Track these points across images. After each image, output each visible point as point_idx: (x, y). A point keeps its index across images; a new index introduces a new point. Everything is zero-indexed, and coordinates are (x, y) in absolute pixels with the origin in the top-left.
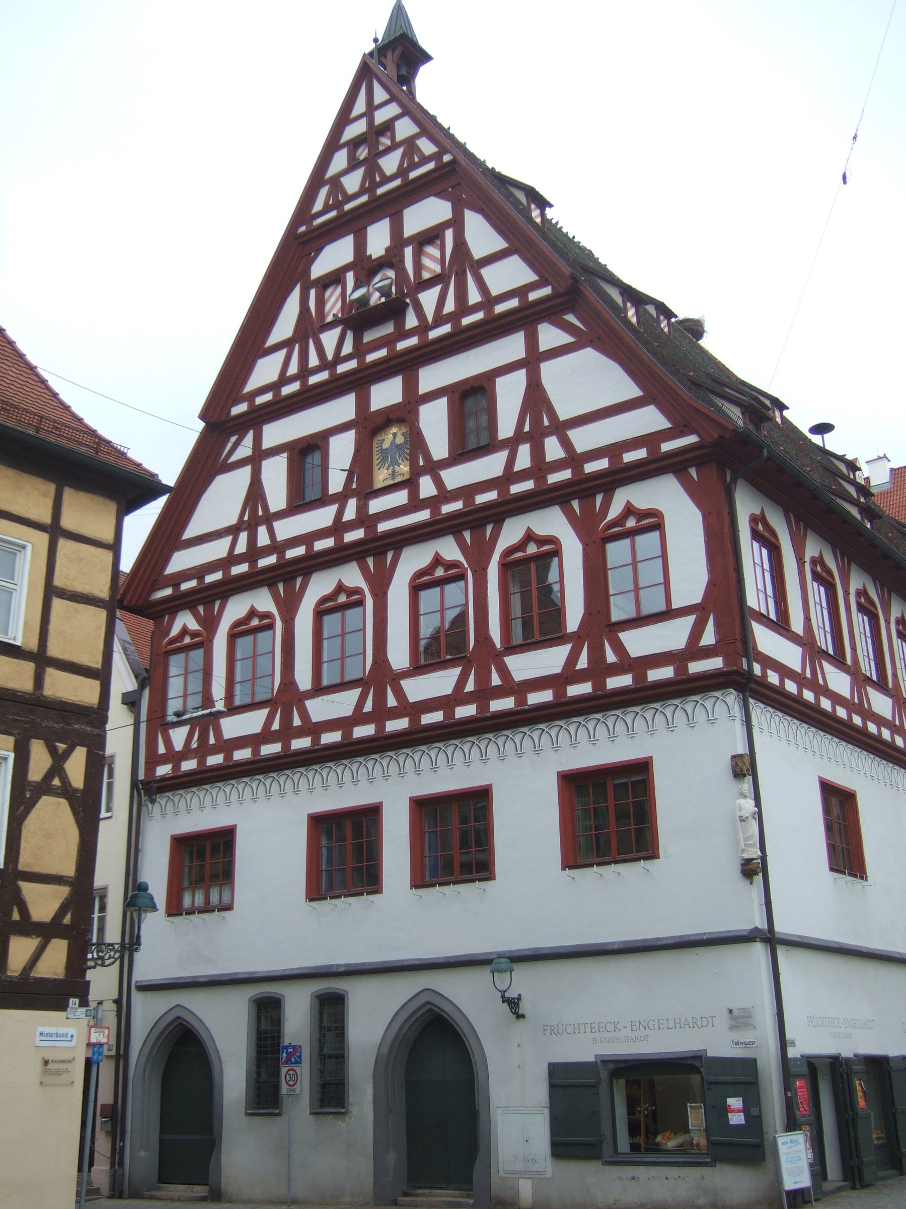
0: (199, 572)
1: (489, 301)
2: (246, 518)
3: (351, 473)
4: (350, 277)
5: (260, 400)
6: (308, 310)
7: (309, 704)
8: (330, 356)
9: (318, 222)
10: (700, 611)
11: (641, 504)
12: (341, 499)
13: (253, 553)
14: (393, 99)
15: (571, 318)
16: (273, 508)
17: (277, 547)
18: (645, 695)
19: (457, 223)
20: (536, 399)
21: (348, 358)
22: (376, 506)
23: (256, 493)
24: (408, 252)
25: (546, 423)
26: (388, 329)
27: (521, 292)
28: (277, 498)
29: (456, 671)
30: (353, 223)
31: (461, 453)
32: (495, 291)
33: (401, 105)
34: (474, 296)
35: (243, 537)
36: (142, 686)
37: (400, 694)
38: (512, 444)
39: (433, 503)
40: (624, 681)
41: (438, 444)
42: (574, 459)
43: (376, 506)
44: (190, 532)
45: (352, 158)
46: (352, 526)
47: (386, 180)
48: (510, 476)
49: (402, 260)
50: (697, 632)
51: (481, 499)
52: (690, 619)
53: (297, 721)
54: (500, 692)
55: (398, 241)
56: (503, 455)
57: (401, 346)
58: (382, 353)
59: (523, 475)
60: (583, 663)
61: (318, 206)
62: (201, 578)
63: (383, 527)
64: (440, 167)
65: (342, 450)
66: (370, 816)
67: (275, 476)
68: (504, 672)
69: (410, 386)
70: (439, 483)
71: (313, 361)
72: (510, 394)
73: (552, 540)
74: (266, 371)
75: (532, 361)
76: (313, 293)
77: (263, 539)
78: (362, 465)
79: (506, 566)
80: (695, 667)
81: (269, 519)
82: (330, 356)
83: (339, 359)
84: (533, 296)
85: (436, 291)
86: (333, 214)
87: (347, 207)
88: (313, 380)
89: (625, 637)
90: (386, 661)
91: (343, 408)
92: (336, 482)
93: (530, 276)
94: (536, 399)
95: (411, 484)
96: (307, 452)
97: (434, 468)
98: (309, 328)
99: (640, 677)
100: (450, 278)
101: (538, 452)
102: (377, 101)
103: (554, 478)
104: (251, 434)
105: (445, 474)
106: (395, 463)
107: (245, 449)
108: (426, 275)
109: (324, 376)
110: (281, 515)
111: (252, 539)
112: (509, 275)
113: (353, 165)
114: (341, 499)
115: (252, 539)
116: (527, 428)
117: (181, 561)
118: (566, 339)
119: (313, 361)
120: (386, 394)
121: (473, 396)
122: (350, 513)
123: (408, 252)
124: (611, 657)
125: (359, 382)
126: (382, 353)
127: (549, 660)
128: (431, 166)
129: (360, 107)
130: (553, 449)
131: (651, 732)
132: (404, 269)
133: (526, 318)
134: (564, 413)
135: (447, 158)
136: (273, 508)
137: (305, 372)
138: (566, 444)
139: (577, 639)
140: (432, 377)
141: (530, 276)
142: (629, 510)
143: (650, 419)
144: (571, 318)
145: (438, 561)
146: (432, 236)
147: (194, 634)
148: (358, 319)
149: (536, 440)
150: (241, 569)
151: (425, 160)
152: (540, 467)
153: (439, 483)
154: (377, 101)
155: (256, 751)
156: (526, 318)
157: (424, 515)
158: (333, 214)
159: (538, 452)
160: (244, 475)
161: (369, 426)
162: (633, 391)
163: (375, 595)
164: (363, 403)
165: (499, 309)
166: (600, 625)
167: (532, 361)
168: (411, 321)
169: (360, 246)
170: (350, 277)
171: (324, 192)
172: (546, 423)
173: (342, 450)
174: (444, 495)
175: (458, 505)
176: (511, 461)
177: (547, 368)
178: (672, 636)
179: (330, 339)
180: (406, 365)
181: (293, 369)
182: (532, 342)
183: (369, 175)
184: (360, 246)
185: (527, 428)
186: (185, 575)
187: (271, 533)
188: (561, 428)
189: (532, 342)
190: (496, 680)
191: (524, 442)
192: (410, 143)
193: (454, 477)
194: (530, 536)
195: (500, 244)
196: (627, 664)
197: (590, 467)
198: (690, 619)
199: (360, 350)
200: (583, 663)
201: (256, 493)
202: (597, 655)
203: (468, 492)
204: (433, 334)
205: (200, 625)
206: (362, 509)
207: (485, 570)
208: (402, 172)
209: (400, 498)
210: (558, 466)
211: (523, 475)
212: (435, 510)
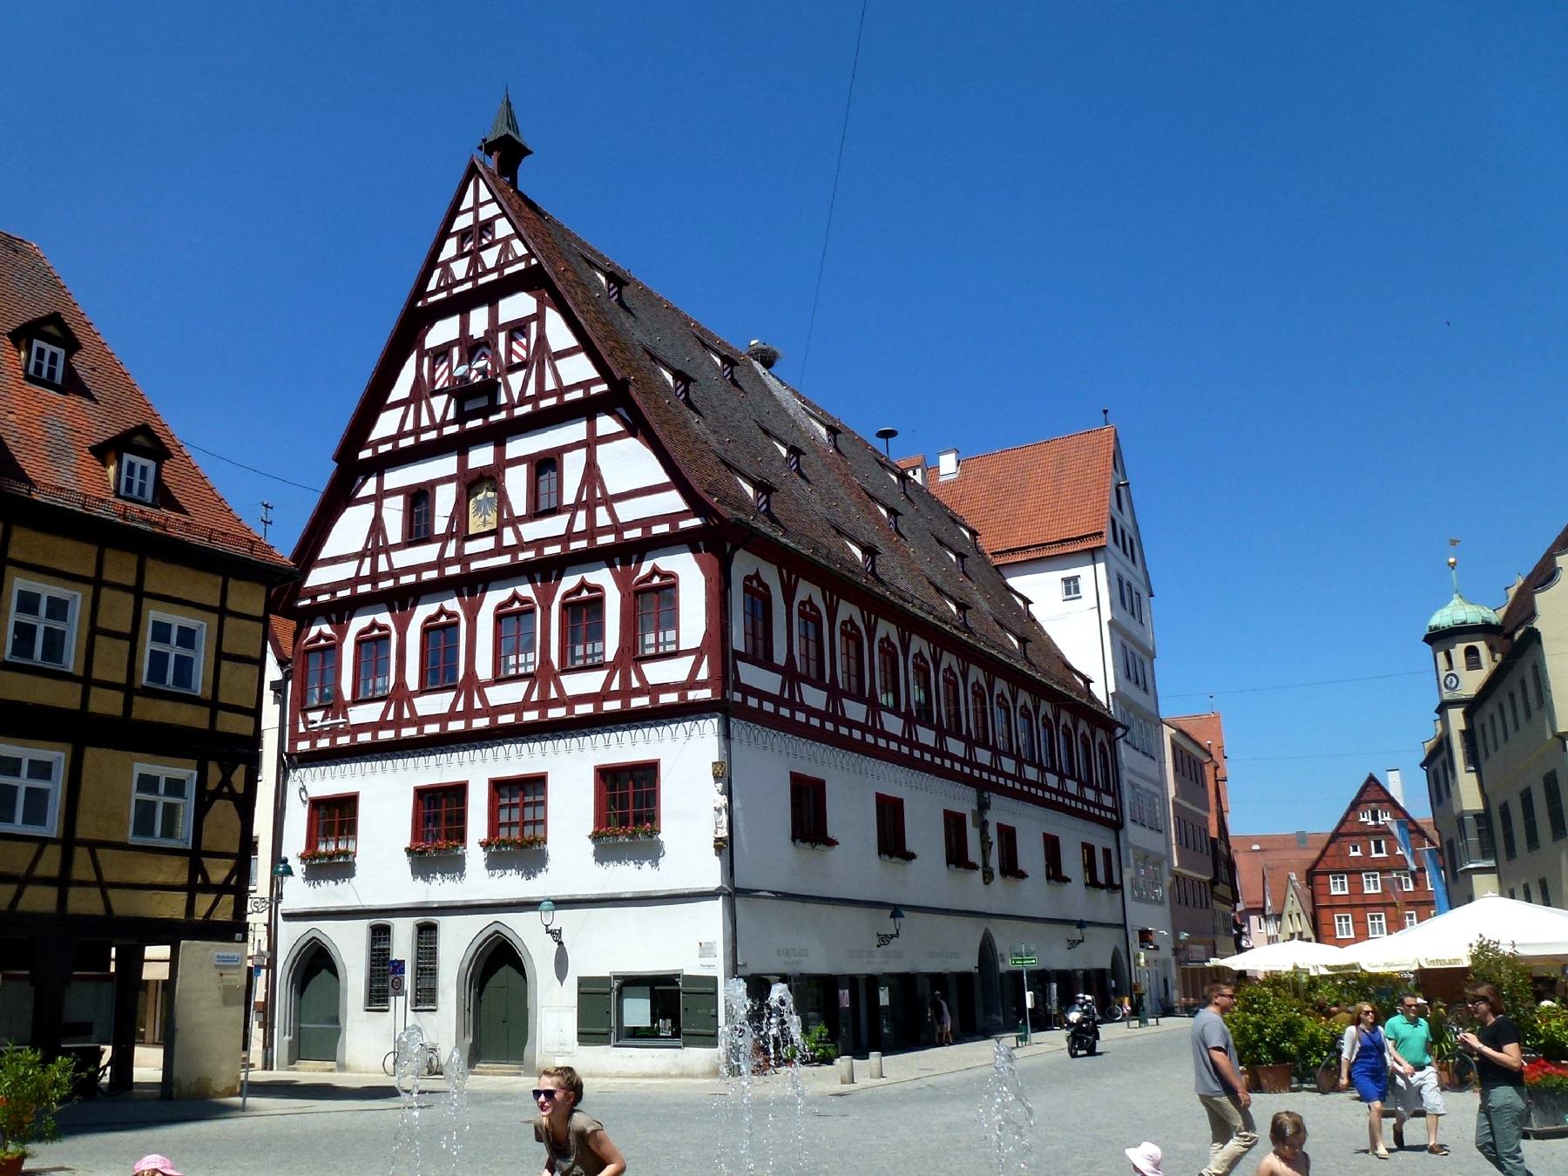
0: (333, 588)
1: (561, 390)
3: (452, 519)
4: (456, 351)
5: (382, 449)
7: (416, 701)
9: (430, 300)
10: (698, 652)
12: (445, 538)
13: (375, 577)
14: (494, 199)
16: (391, 542)
17: (394, 574)
19: (539, 317)
20: (592, 474)
23: (377, 526)
24: (502, 336)
27: (585, 385)
28: (394, 533)
30: (460, 306)
31: (535, 513)
33: (501, 206)
34: (550, 385)
35: (368, 561)
36: (286, 677)
37: (483, 699)
39: (513, 550)
42: (617, 528)
43: (471, 547)
44: (325, 553)
45: (460, 246)
46: (450, 562)
47: (487, 272)
49: (496, 344)
51: (550, 551)
52: (692, 658)
53: (406, 715)
55: (494, 326)
56: (566, 517)
58: (479, 422)
59: (580, 536)
60: (615, 686)
61: (432, 286)
62: (334, 593)
63: (475, 565)
64: (529, 270)
65: (445, 498)
66: (458, 792)
67: (394, 512)
69: (500, 454)
70: (518, 534)
71: (425, 422)
73: (598, 588)
75: (591, 443)
77: (383, 566)
78: (460, 512)
79: (564, 607)
80: (692, 695)
81: (388, 549)
83: (445, 423)
84: (594, 390)
85: (521, 374)
86: (443, 295)
87: (456, 291)
88: (424, 437)
91: (447, 465)
92: (440, 526)
94: (592, 474)
95: (496, 533)
96: (419, 497)
97: (515, 522)
98: (421, 391)
99: (654, 700)
101: (591, 518)
102: (481, 200)
103: (602, 540)
105: (522, 527)
106: (486, 513)
107: (370, 488)
108: (516, 360)
109: (433, 435)
110: (397, 547)
111: (374, 565)
113: (460, 255)
114: (445, 538)
115: (374, 565)
117: (317, 577)
119: (425, 422)
120: (481, 457)
121: (545, 465)
122: (450, 552)
123: (502, 336)
124: (635, 684)
125: (460, 445)
126: (479, 422)
127: (592, 682)
128: (521, 266)
129: (468, 202)
130: (602, 518)
131: (661, 741)
132: (497, 353)
133: (587, 409)
135: (534, 261)
139: (613, 667)
140: (517, 447)
141: (593, 373)
142: (655, 571)
144: (621, 411)
145: (515, 597)
146: (517, 329)
147: (328, 638)
148: (461, 392)
149: (590, 507)
150: (364, 589)
151: (518, 260)
153: (518, 534)
154: (481, 200)
155: (375, 736)
157: (505, 560)
158: (443, 295)
159: (591, 518)
160: (368, 510)
162: (664, 478)
163: (468, 620)
164: (462, 463)
165: (568, 397)
166: (631, 656)
168: (503, 400)
169: (464, 326)
170: (456, 351)
171: (437, 273)
173: (445, 498)
176: (571, 523)
178: (677, 670)
179: (439, 403)
180: (498, 436)
181: (409, 426)
183: (473, 265)
184: (464, 326)
186: (320, 590)
188: (609, 501)
190: (553, 694)
192: (506, 241)
194: (583, 585)
195: (572, 342)
197: (628, 535)
198: (692, 658)
199: (461, 418)
200: (615, 686)
201: (377, 526)
202: (625, 680)
203: (539, 544)
204: (519, 412)
206: (460, 549)
207: (549, 608)
208: (499, 267)
209: (488, 543)
210: (605, 531)
211: (580, 536)
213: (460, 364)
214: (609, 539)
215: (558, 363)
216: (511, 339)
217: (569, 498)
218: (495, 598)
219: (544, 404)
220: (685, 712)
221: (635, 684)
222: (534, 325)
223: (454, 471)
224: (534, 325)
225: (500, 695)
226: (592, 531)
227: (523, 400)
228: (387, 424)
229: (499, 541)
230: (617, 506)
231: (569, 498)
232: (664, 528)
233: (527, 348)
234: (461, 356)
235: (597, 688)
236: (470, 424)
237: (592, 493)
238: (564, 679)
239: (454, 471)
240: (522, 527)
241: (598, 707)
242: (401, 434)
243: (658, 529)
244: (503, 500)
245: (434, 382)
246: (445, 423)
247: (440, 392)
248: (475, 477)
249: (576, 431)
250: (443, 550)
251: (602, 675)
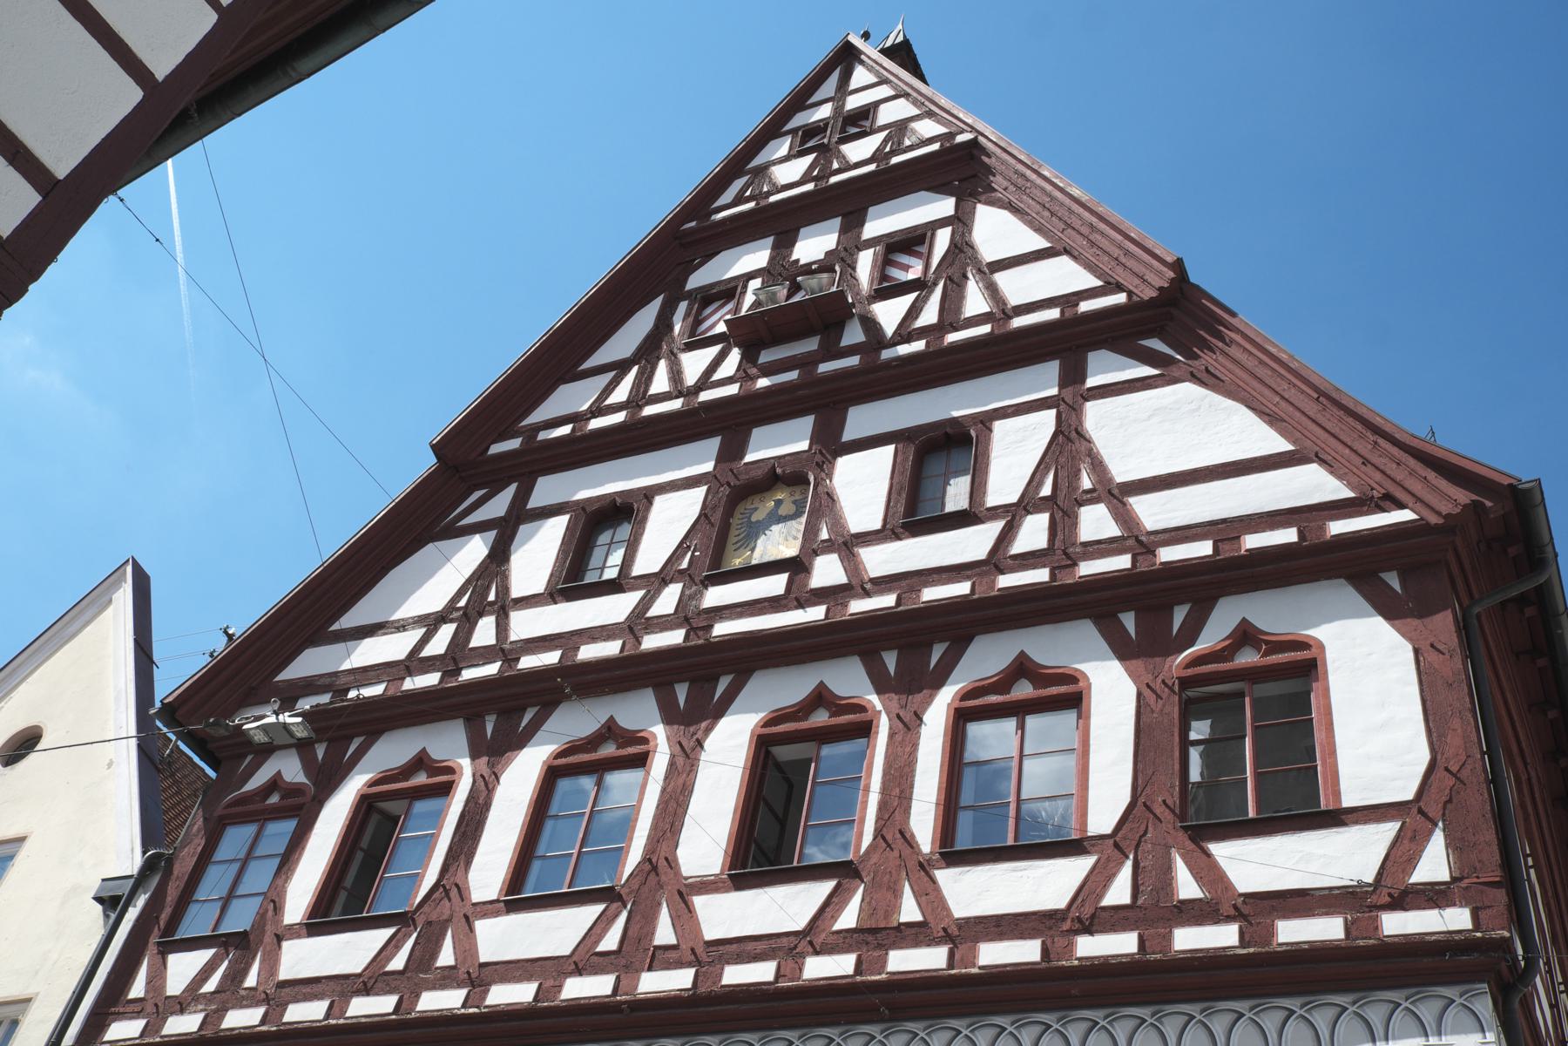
2: (462, 603)
15: (1156, 344)
16: (517, 591)
17: (505, 651)
26: (811, 345)
38: (1013, 515)
42: (1138, 541)
54: (915, 935)
56: (993, 529)
68: (930, 897)
74: (573, 397)
84: (1085, 306)
89: (1221, 851)
90: (672, 863)
93: (1087, 280)
97: (848, 545)
107: (498, 506)
116: (1046, 490)
134: (1122, 471)
136: (517, 591)
147: (294, 790)
156: (1067, 341)
174: (859, 585)
187: (502, 628)
188: (1117, 495)
200: (1119, 892)
205: (307, 774)
237: (1066, 482)
250: (645, 604)
251: (1074, 870)
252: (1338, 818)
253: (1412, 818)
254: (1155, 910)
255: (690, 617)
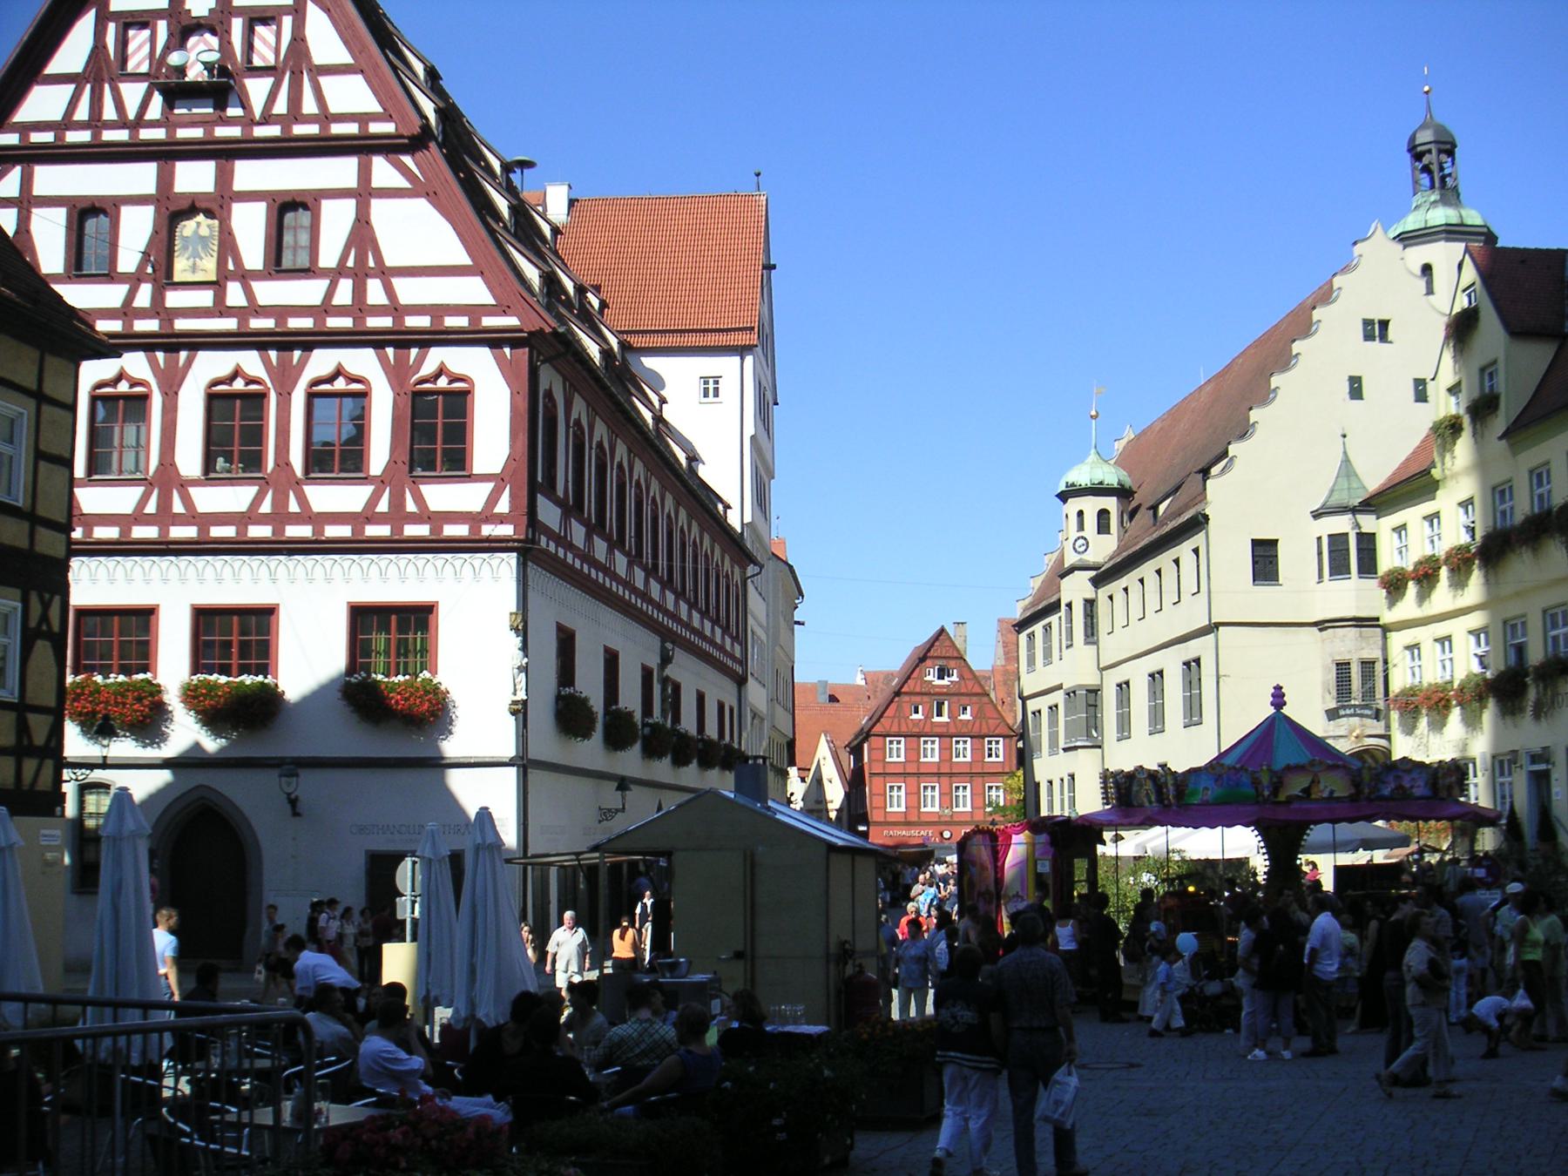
1: (325, 117)
4: (162, 27)
6: (105, 47)
8: (131, 115)
11: (455, 368)
12: (135, 280)
18: (436, 546)
20: (362, 235)
21: (153, 124)
22: (174, 299)
24: (237, 25)
25: (371, 263)
29: (252, 491)
32: (334, 108)
34: (309, 106)
39: (241, 313)
40: (422, 530)
41: (253, 254)
42: (395, 309)
43: (174, 299)
46: (143, 314)
48: (326, 308)
49: (228, 32)
50: (493, 499)
51: (295, 323)
52: (490, 486)
54: (297, 519)
56: (322, 285)
57: (221, 132)
59: (341, 311)
63: (181, 325)
65: (136, 228)
71: (109, 113)
72: (337, 220)
75: (364, 193)
76: (112, 27)
80: (487, 530)
82: (131, 115)
83: (140, 122)
85: (267, 83)
88: (108, 136)
91: (140, 177)
92: (128, 261)
94: (362, 235)
95: (218, 286)
97: (245, 277)
98: (102, 70)
99: (437, 529)
100: (284, 73)
101: (359, 292)
103: (373, 322)
104: (18, 170)
105: (257, 287)
108: (257, 62)
112: (351, 96)
114: (135, 280)
116: (350, 263)
118: (401, 182)
123: (237, 25)
124: (411, 507)
125: (167, 154)
130: (375, 293)
132: (226, 46)
133: (363, 147)
137: (95, 122)
138: (389, 290)
139: (381, 482)
143: (475, 291)
149: (360, 277)
152: (359, 307)
157: (230, 324)
159: (359, 292)
161: (174, 211)
163: (165, 394)
165: (337, 129)
167: (364, 193)
170: (162, 27)
172: (371, 263)
173: (136, 228)
175: (268, 323)
177: (377, 205)
179: (133, 93)
180: (225, 154)
182: (365, 173)
185: (350, 263)
188: (386, 274)
189: (365, 173)
191: (347, 277)
193: (270, 292)
195: (345, 57)
196: (425, 516)
197: (412, 322)
198: (490, 486)
202: (397, 502)
203: (281, 312)
204: (260, 132)
206: (158, 297)
209: (205, 298)
210: (378, 311)
211: (341, 311)
212: (243, 321)
213: (168, 49)
214: (386, 322)
215: (325, 81)
216: (249, 32)
217: (328, 257)
218: (209, 366)
219: (299, 130)
220: (475, 545)
221: (411, 507)
222: (287, 22)
223: (150, 188)
224: (287, 22)
225: (210, 499)
226: (359, 307)
227: (267, 119)
228: (42, 104)
229: (220, 296)
230: (398, 283)
231: (328, 257)
232: (462, 322)
233: (277, 51)
234: (171, 35)
235: (357, 507)
236: (183, 133)
238: (310, 490)
239: (150, 188)
240: (257, 287)
241: (358, 529)
242: (67, 123)
243: (451, 322)
244: (227, 245)
245: (124, 59)
246: (140, 122)
247: (136, 77)
248: (185, 205)
249: (343, 171)
252: (471, 478)
253: (499, 480)
254: (397, 516)
255: (157, 309)
